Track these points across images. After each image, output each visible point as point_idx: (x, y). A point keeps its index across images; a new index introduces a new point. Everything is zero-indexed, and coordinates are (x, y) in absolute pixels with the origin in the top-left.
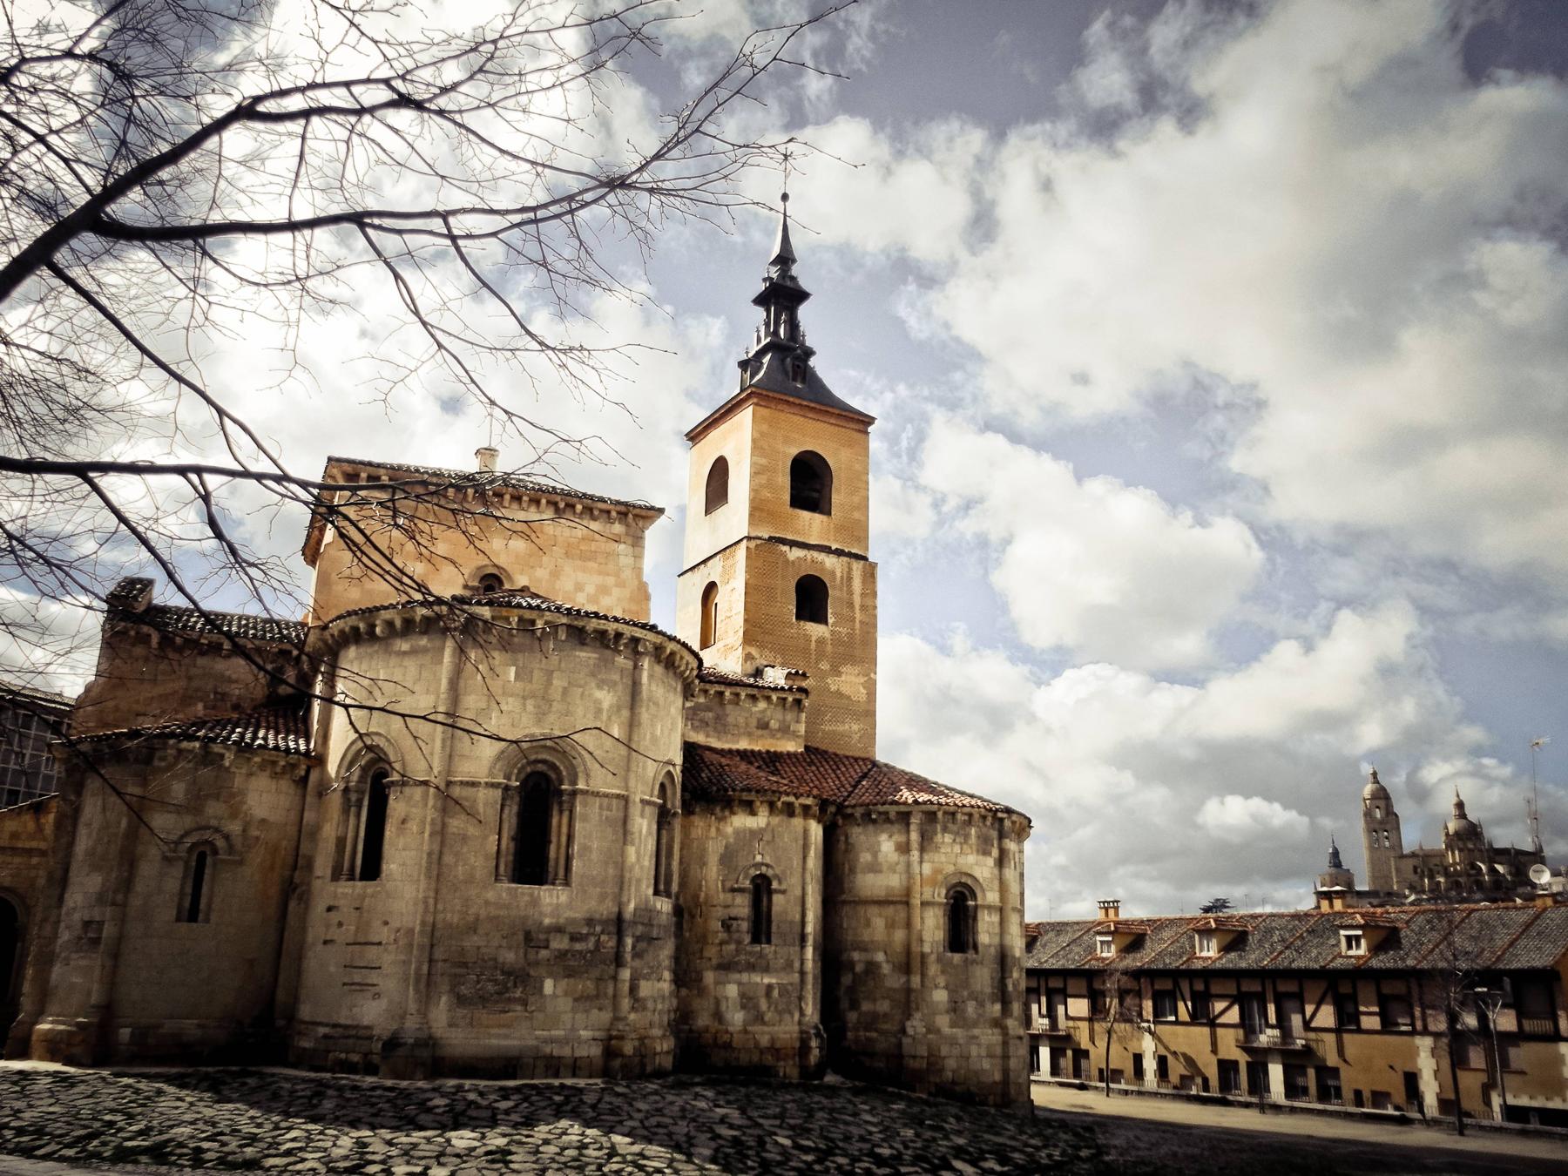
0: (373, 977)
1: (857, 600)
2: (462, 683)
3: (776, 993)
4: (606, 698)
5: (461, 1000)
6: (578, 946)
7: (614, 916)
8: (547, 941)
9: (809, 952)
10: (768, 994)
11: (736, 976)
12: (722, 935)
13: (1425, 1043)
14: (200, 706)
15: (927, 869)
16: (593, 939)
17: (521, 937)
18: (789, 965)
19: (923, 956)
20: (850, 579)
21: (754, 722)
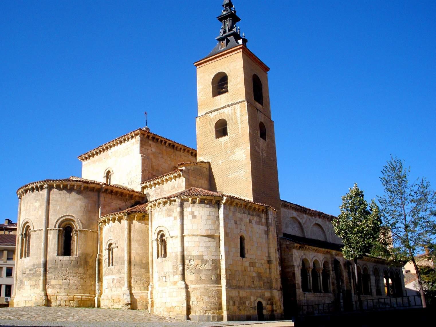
1: (239, 120)
3: (115, 281)
4: (37, 204)
6: (31, 272)
9: (126, 266)
16: (34, 270)
18: (119, 272)
20: (235, 113)
21: (170, 188)
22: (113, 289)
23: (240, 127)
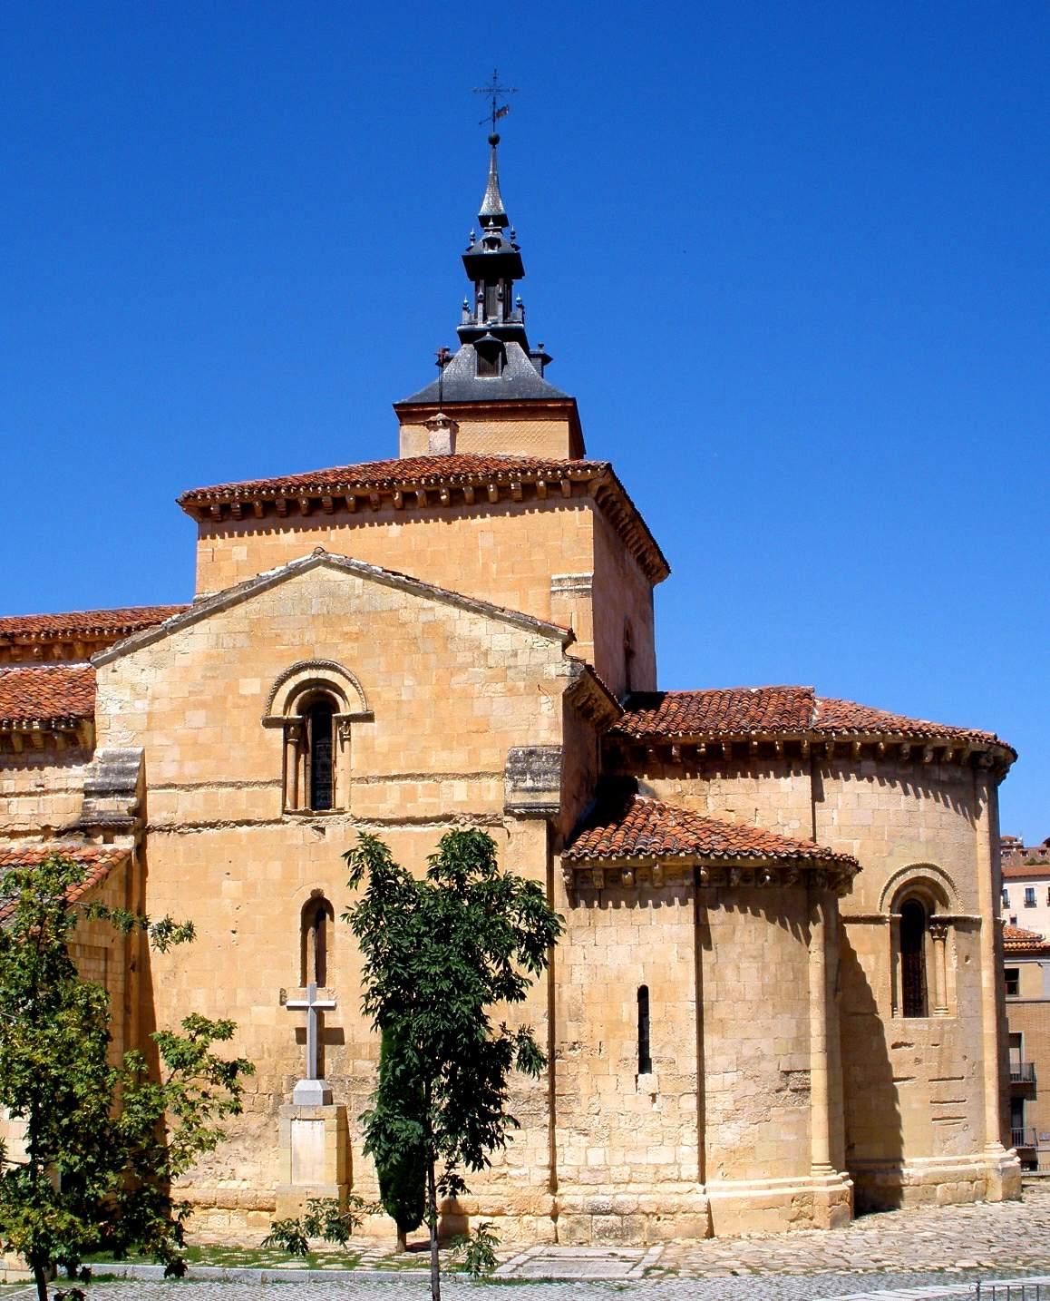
0: (959, 1110)
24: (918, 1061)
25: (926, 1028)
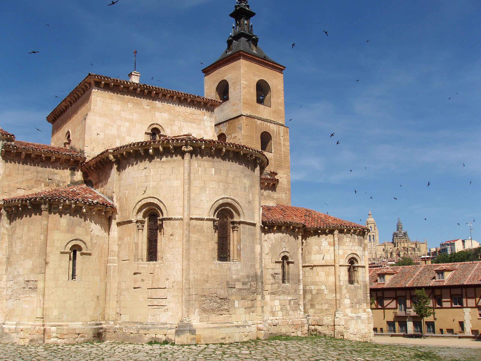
0: (163, 302)
1: (282, 142)
2: (192, 175)
3: (292, 303)
5: (204, 310)
7: (254, 274)
8: (235, 285)
10: (290, 304)
11: (278, 297)
12: (272, 280)
13: (467, 311)
14: (43, 185)
15: (341, 252)
16: (249, 284)
17: (225, 283)
19: (341, 286)
22: (291, 312)
23: (283, 149)
24: (143, 280)
25: (147, 266)
